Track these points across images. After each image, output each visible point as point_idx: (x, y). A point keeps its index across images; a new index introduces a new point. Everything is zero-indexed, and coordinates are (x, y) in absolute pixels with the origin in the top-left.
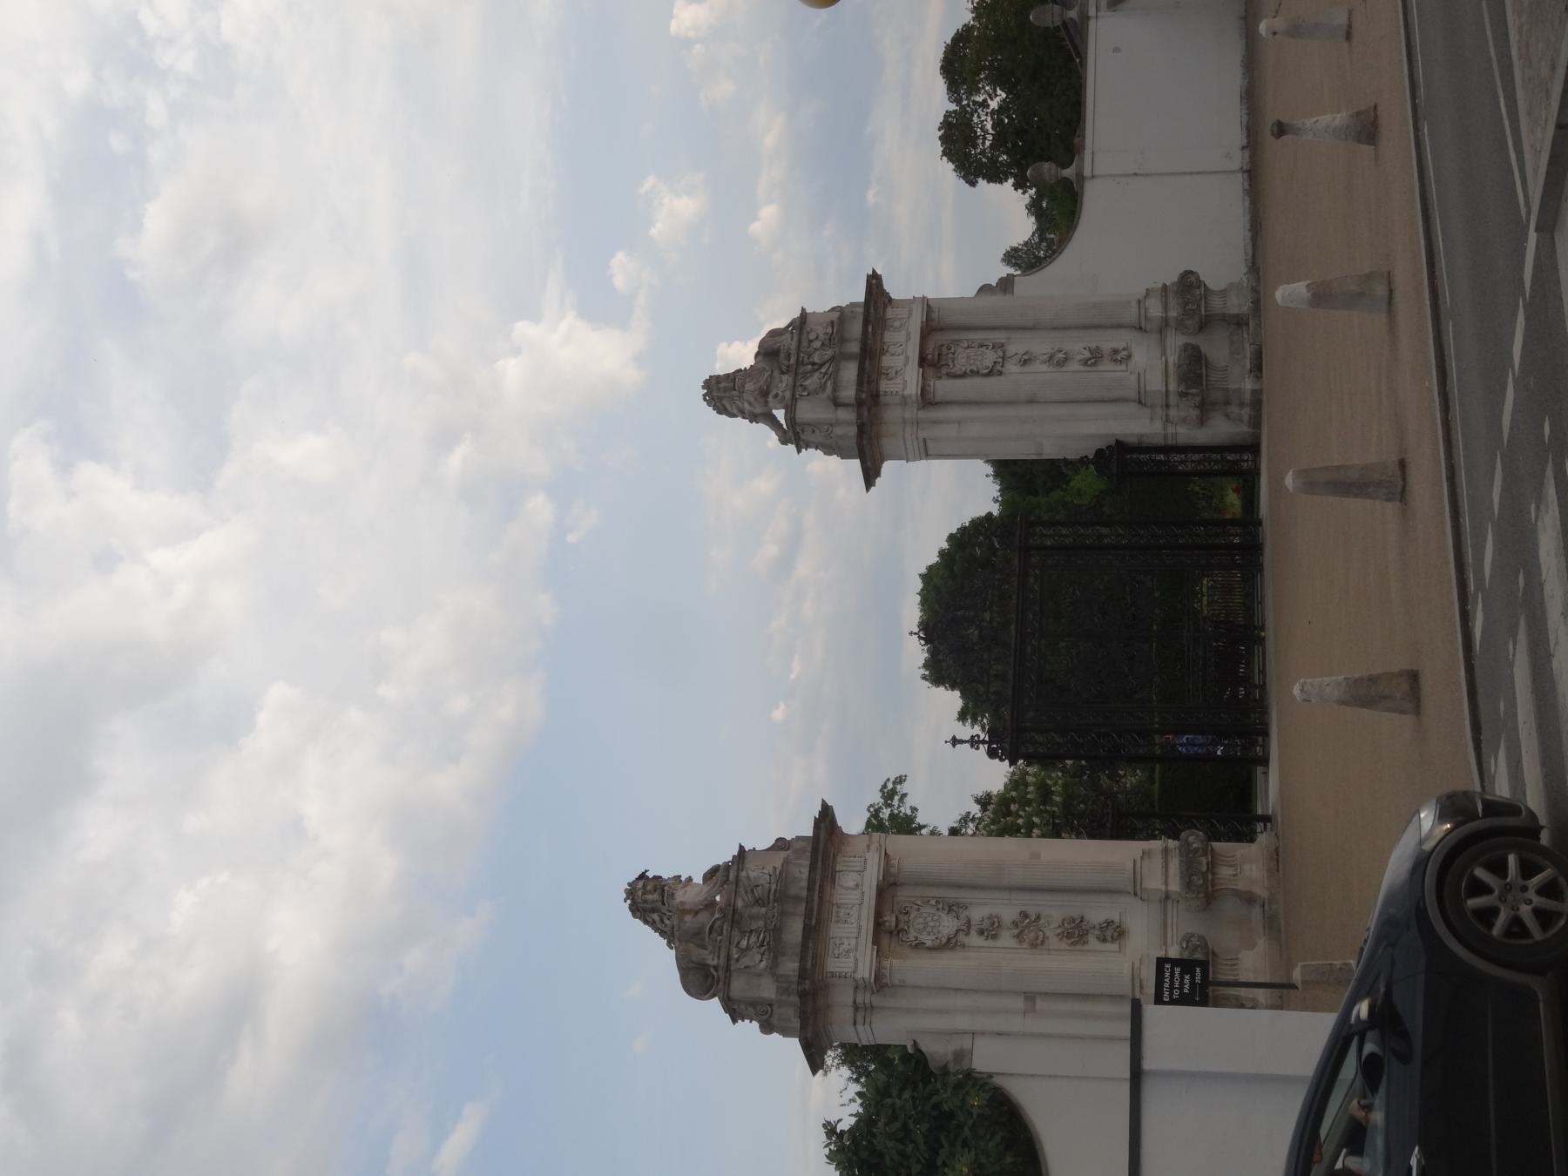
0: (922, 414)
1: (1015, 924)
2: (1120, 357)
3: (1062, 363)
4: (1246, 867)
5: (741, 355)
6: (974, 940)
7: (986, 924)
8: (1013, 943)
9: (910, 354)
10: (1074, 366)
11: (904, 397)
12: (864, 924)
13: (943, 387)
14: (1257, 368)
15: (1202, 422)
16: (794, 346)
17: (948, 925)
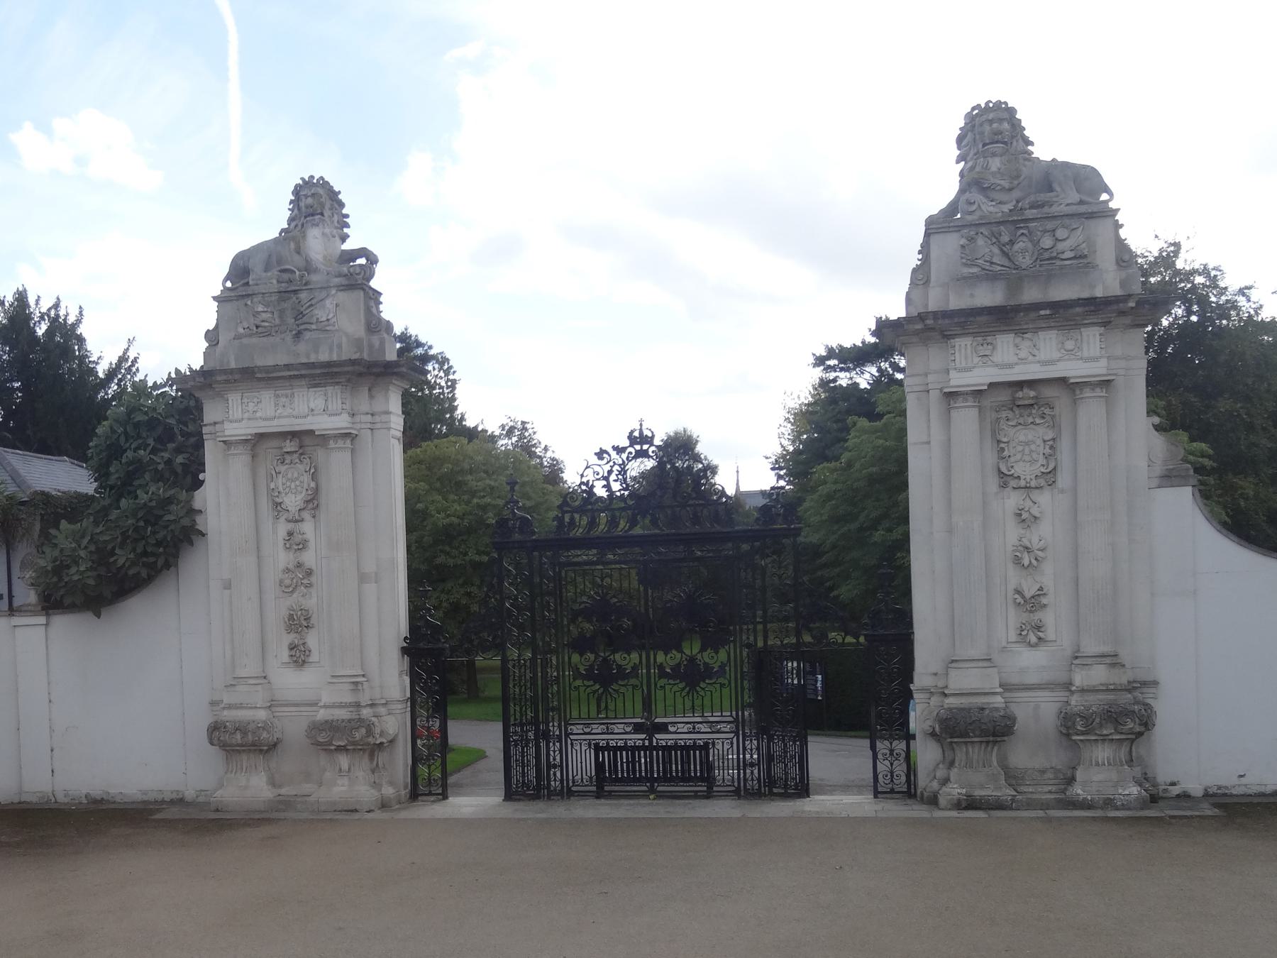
0: (935, 395)
1: (299, 565)
2: (1032, 634)
3: (1017, 561)
4: (345, 781)
5: (1049, 142)
6: (283, 529)
7: (298, 538)
8: (282, 566)
9: (1017, 369)
10: (1014, 578)
11: (948, 371)
12: (275, 422)
13: (966, 418)
16: (1055, 210)
17: (293, 502)
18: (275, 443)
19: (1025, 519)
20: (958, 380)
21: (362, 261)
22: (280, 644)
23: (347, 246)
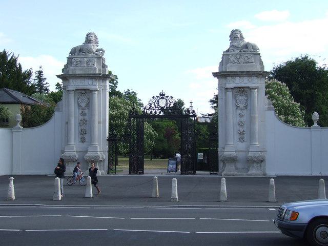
1: (84, 119)
3: (239, 124)
5: (248, 39)
6: (80, 111)
8: (80, 119)
17: (83, 105)
18: (79, 91)
19: (241, 116)
20: (228, 86)
21: (101, 51)
23: (99, 48)
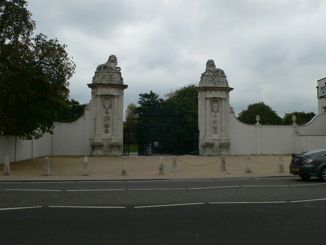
2: (215, 132)
5: (218, 66)
13: (208, 102)
14: (209, 155)
15: (202, 146)
17: (107, 106)
20: (207, 96)
22: (103, 129)
23: (117, 66)
